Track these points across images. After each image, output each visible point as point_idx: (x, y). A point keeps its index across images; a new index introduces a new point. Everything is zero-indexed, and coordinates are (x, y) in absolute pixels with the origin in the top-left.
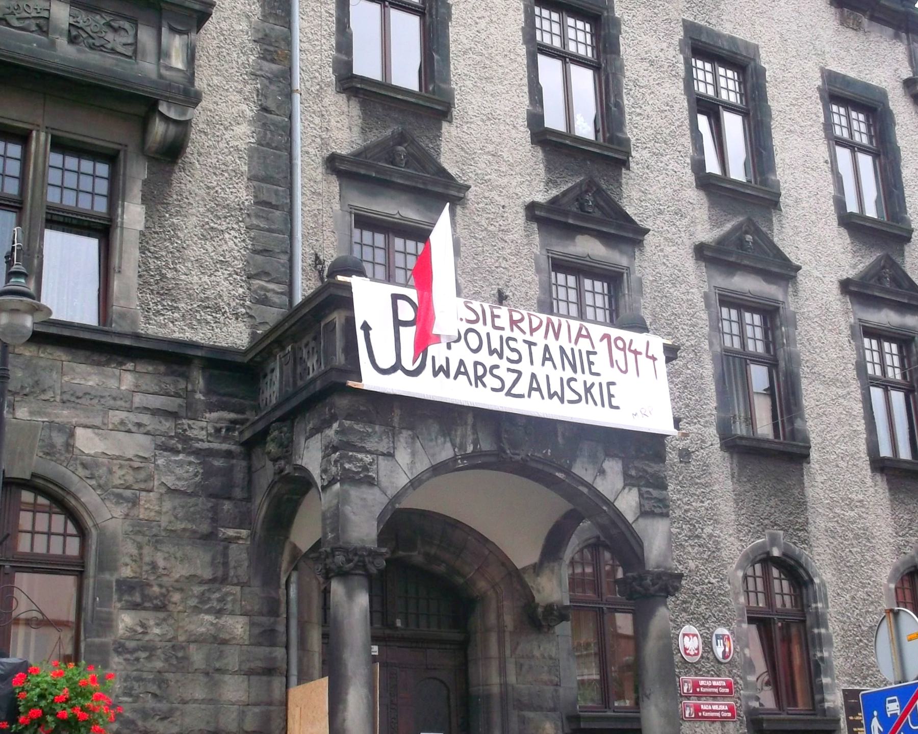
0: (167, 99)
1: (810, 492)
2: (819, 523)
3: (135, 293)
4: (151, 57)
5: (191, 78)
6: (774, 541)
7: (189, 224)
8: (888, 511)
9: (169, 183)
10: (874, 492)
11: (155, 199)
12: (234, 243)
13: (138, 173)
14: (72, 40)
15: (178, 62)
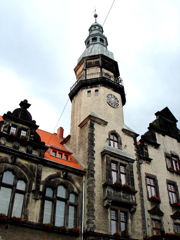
0: (134, 205)
3: (131, 233)
4: (131, 199)
5: (136, 202)
7: (135, 222)
9: (133, 216)
11: (132, 219)
12: (140, 224)
13: (129, 215)
14: (123, 198)
15: (134, 200)
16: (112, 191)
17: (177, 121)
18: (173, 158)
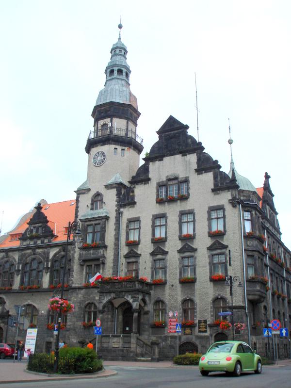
1: (196, 288)
2: (197, 292)
6: (188, 297)
8: (212, 288)
10: (210, 285)
14: (93, 254)
16: (84, 252)
17: (187, 127)
18: (170, 183)
